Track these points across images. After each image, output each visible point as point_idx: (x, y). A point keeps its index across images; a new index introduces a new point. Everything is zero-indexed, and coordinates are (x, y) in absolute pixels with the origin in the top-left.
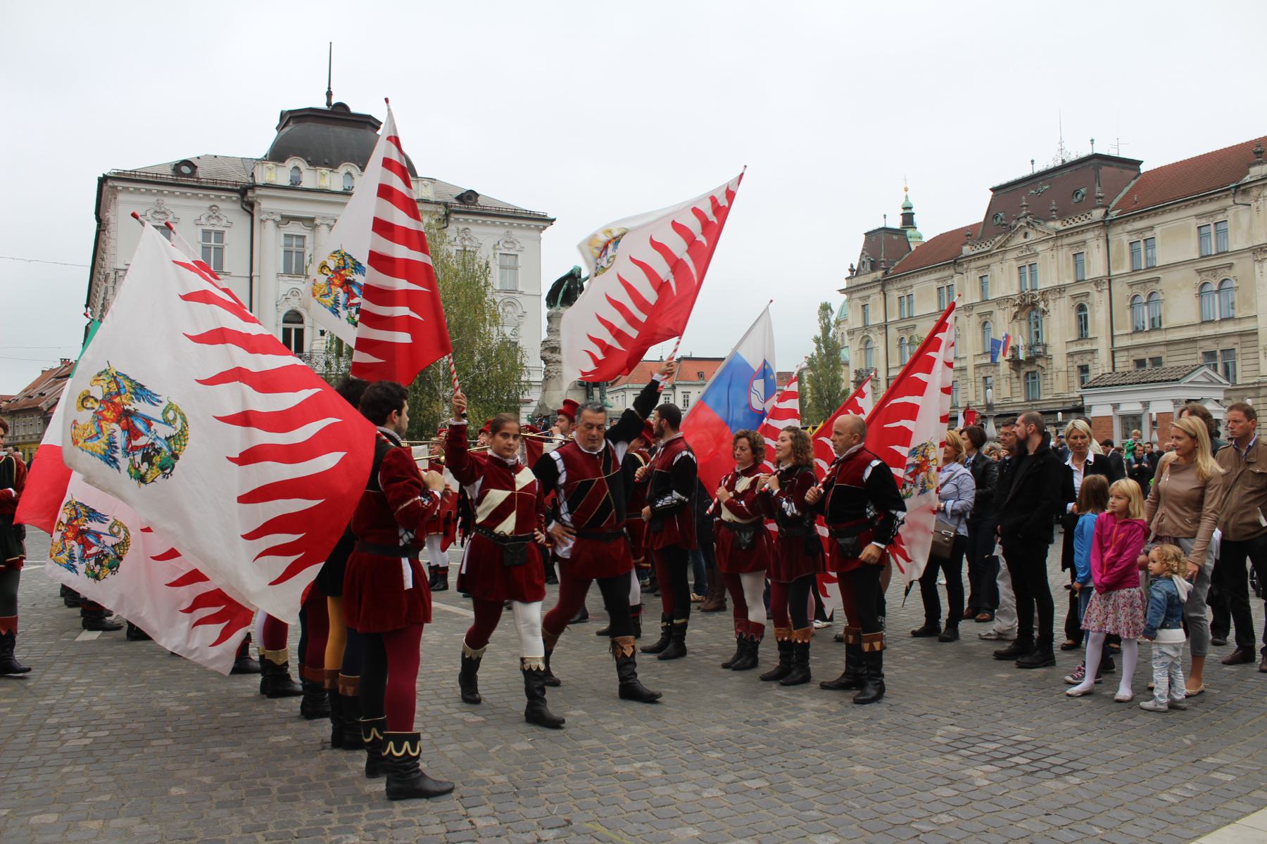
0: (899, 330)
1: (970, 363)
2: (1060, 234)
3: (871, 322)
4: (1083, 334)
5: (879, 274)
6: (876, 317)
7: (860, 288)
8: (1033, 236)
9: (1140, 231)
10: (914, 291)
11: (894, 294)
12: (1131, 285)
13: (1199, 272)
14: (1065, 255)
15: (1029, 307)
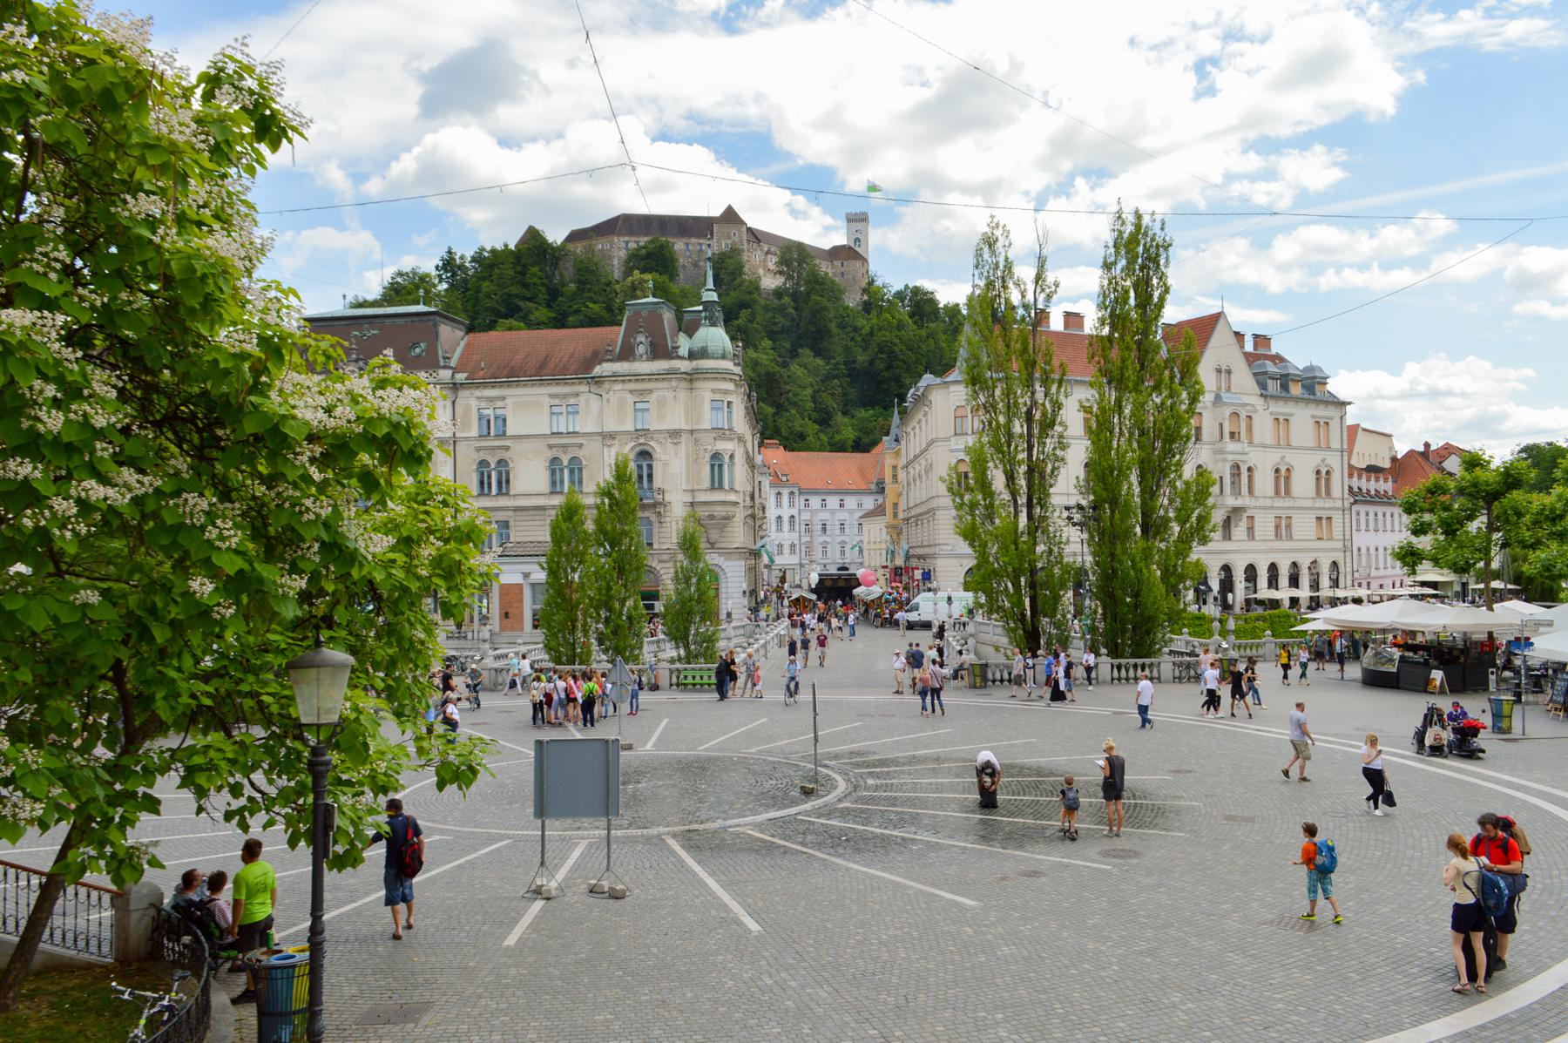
9: (492, 399)
12: (478, 450)
13: (550, 447)
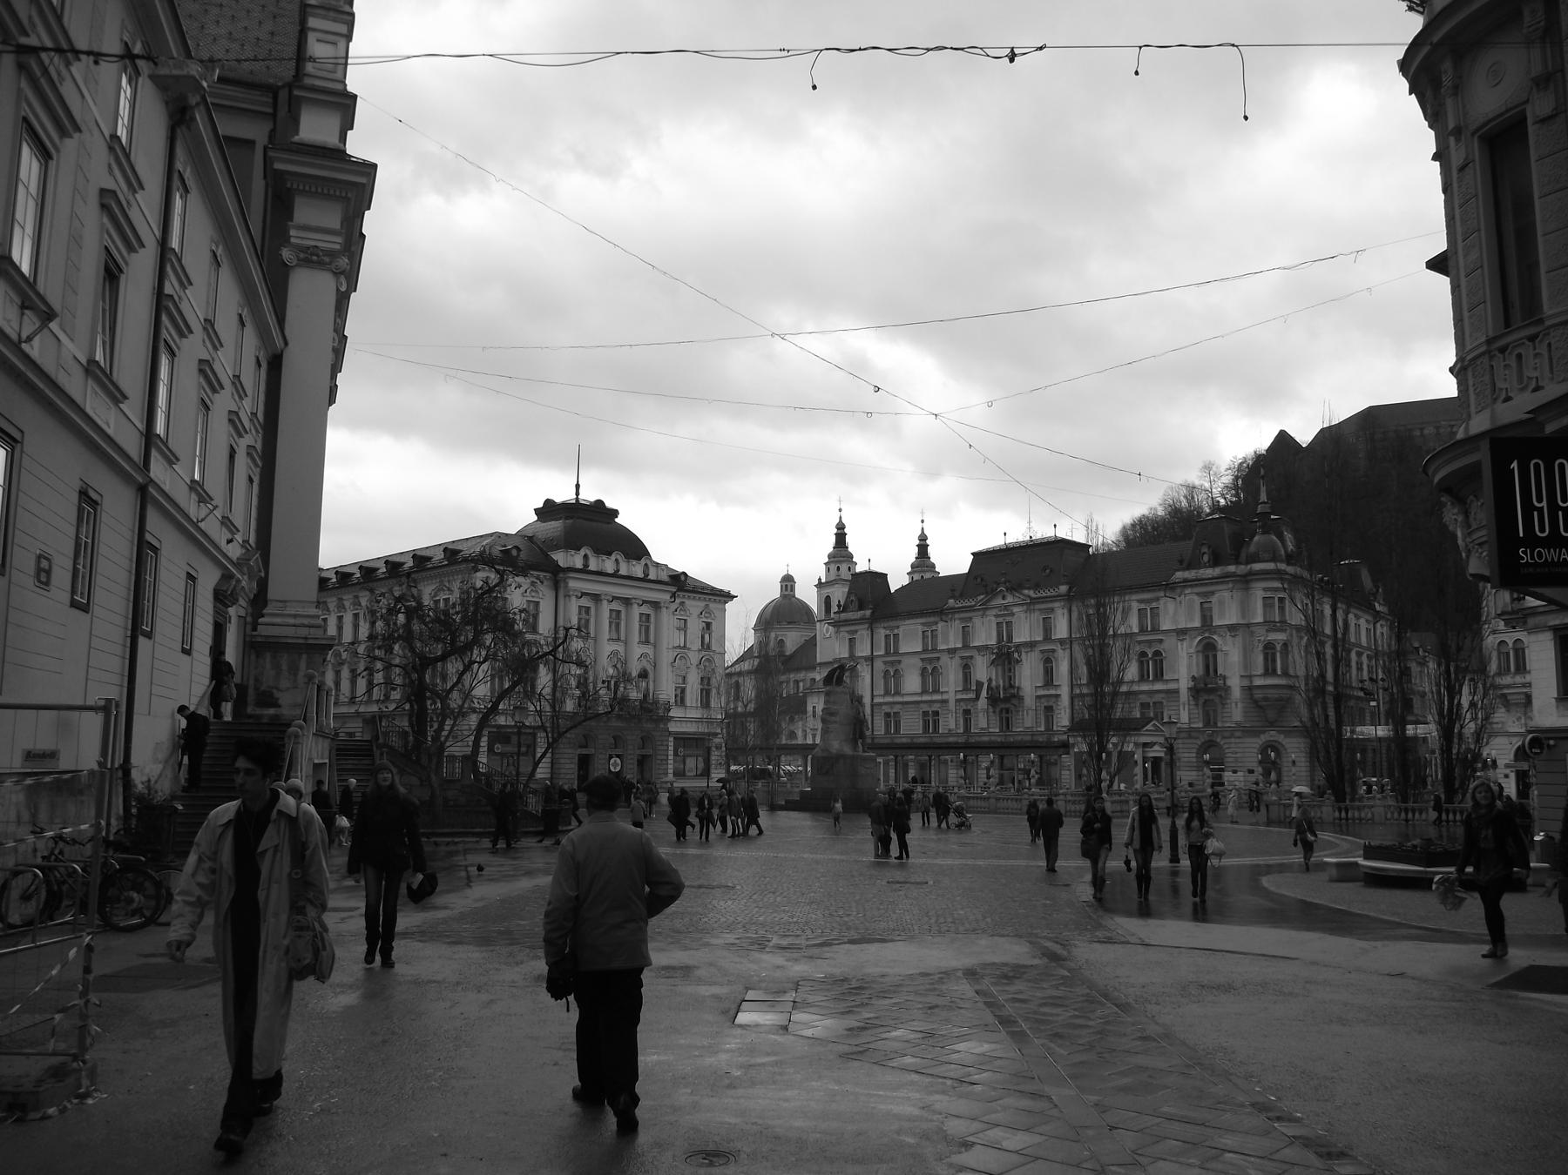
0: (885, 663)
1: (951, 697)
2: (1034, 601)
3: (859, 654)
4: (1049, 680)
5: (868, 613)
6: (863, 650)
7: (847, 622)
8: (1010, 599)
10: (900, 631)
11: (881, 633)
14: (1037, 617)
15: (1005, 656)
